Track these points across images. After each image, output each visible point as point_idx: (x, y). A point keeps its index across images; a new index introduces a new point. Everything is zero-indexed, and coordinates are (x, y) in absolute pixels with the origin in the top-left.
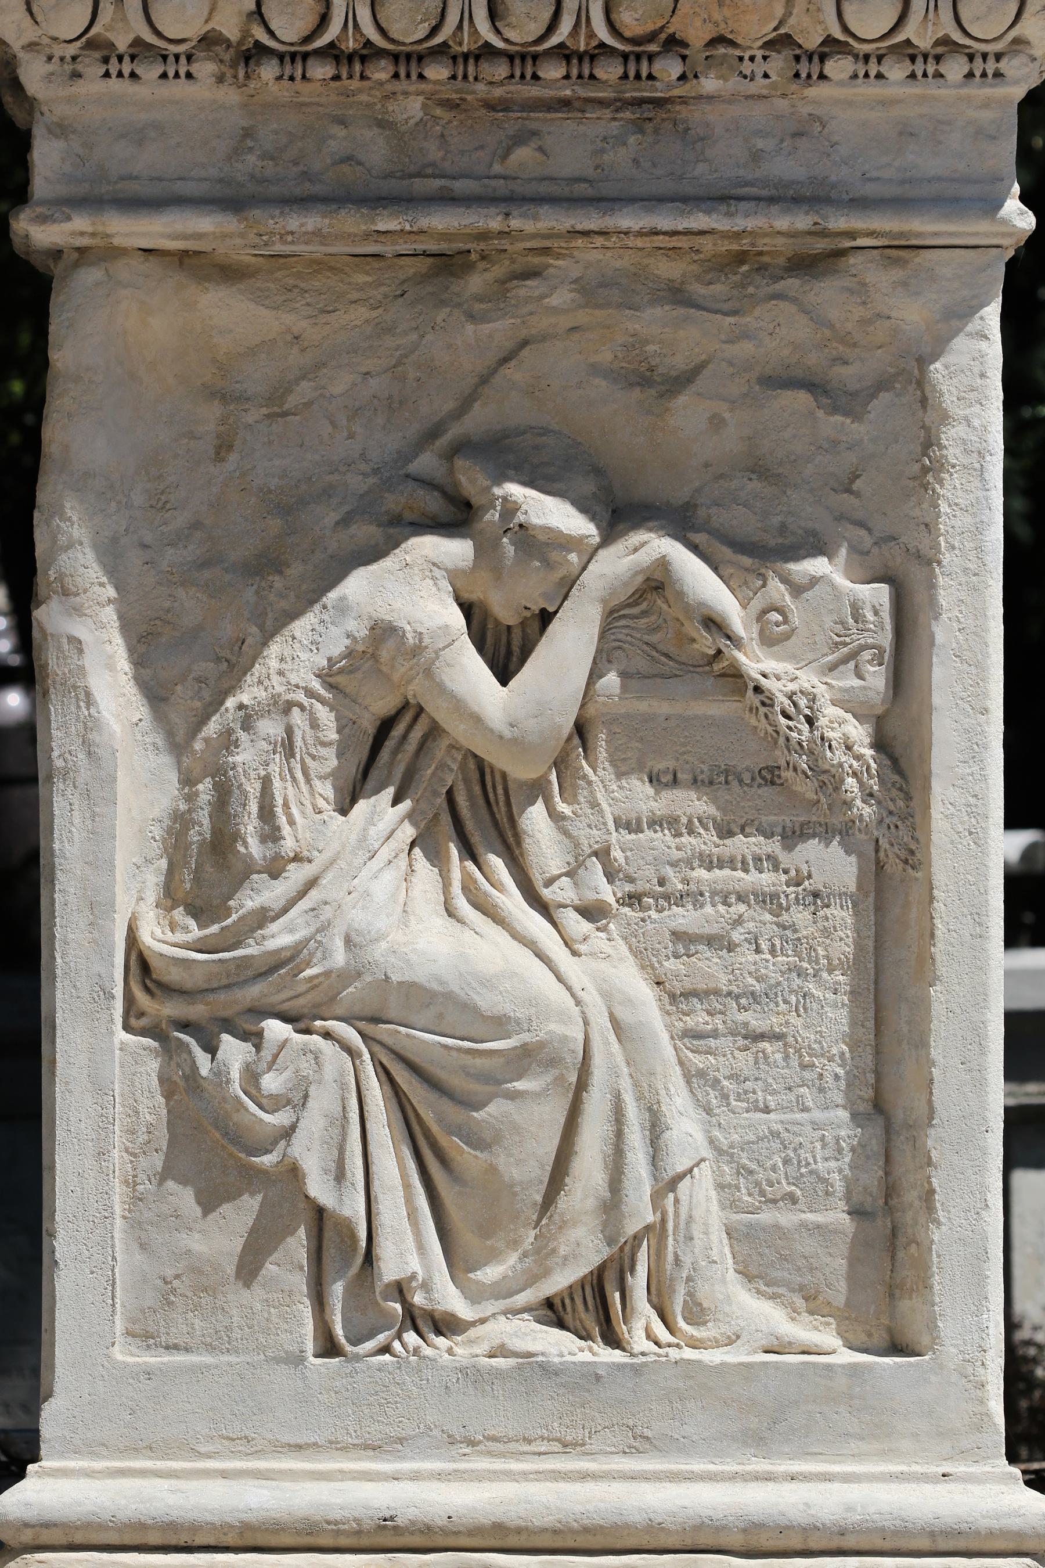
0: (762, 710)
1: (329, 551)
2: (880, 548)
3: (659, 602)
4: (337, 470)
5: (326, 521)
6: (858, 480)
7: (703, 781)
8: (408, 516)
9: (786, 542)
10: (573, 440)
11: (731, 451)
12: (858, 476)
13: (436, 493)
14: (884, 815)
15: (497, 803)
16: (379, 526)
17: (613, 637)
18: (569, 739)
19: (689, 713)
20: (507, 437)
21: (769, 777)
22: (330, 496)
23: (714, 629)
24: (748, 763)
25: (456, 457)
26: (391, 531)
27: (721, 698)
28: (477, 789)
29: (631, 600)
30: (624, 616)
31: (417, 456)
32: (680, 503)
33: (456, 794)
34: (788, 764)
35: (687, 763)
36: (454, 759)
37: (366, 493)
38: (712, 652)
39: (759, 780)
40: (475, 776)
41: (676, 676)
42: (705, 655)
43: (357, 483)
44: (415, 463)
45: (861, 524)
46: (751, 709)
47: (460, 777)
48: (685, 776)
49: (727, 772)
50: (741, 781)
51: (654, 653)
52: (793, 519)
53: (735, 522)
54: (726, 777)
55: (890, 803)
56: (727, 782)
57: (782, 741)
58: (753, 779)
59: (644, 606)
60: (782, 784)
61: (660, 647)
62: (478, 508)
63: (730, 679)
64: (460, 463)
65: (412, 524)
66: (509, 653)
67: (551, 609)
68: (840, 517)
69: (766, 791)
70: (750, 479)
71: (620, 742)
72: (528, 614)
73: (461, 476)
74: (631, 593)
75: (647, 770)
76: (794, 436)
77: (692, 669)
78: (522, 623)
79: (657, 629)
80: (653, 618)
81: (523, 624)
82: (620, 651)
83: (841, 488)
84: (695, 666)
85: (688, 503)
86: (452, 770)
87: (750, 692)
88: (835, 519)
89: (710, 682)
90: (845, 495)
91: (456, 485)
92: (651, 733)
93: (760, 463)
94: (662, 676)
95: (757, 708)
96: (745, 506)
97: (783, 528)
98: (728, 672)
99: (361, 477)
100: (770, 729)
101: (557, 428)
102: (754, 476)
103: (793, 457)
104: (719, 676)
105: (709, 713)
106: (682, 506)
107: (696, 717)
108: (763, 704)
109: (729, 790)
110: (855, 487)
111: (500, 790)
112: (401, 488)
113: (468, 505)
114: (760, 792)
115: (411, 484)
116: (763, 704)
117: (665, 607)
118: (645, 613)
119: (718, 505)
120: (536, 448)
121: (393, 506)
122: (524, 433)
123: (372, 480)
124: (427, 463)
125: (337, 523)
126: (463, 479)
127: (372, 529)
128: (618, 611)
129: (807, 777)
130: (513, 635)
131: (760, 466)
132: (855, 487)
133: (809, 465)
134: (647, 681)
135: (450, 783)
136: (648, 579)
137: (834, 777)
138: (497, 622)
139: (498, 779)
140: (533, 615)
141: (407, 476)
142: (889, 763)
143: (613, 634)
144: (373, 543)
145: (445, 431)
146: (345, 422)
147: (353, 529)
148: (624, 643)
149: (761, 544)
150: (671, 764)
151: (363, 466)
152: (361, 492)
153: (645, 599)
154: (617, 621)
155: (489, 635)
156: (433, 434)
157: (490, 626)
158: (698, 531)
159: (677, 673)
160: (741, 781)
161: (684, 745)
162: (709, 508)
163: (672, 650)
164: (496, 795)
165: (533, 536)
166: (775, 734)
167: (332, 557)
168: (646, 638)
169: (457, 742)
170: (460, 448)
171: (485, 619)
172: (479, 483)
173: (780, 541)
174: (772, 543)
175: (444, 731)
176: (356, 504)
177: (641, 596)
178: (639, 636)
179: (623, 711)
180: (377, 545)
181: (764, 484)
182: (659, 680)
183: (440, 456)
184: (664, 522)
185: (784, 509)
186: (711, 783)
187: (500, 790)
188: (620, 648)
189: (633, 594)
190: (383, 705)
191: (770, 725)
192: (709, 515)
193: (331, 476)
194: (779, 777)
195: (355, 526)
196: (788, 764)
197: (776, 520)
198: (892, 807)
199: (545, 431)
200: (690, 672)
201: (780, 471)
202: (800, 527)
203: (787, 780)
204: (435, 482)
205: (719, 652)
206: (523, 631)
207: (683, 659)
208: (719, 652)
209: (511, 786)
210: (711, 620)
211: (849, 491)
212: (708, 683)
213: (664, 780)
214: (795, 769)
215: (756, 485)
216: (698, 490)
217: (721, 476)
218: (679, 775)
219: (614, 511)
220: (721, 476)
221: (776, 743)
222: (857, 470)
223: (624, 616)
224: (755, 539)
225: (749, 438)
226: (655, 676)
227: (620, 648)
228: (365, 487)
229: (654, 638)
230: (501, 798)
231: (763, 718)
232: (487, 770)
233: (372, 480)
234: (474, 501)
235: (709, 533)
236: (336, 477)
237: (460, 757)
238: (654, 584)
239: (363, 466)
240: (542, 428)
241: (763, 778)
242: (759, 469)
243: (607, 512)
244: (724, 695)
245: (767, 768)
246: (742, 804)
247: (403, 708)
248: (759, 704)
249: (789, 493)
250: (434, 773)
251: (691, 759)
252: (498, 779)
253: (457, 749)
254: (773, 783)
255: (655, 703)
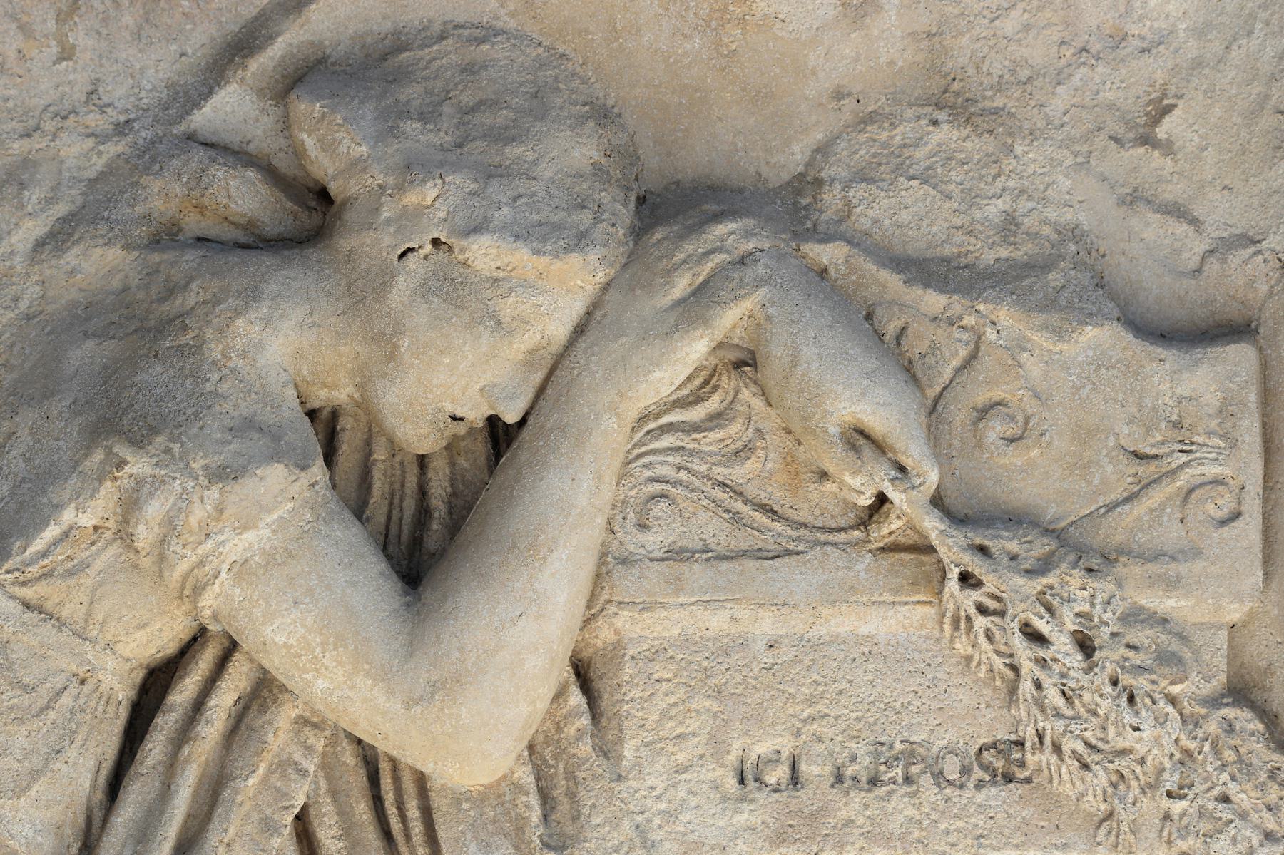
0: (981, 622)
1: (23, 305)
2: (1224, 260)
3: (746, 394)
4: (37, 128)
5: (14, 239)
6: (1167, 118)
7: (855, 778)
8: (194, 224)
9: (1018, 254)
10: (548, 49)
11: (892, 63)
12: (1168, 110)
13: (251, 174)
14: (1255, 842)
15: (408, 837)
16: (126, 247)
17: (648, 473)
18: (560, 695)
19: (820, 631)
20: (402, 48)
21: (1000, 764)
22: (23, 186)
23: (867, 451)
24: (949, 736)
25: (293, 96)
26: (156, 257)
27: (887, 597)
28: (363, 811)
29: (686, 392)
30: (670, 428)
31: (210, 93)
32: (785, 177)
33: (315, 823)
34: (1041, 737)
35: (820, 740)
36: (309, 749)
37: (102, 177)
38: (865, 500)
39: (978, 773)
40: (356, 780)
41: (789, 553)
42: (849, 506)
43: (77, 153)
44: (207, 109)
45: (1178, 212)
46: (956, 622)
47: (323, 785)
48: (816, 770)
49: (910, 756)
50: (939, 776)
51: (739, 506)
52: (1030, 205)
53: (904, 216)
54: (907, 766)
55: (1265, 813)
56: (908, 780)
57: (1027, 687)
58: (966, 770)
59: (714, 404)
60: (1029, 781)
61: (752, 491)
62: (344, 203)
63: (908, 557)
64: (305, 107)
65: (201, 240)
66: (424, 512)
67: (511, 418)
68: (1133, 199)
69: (995, 796)
70: (935, 123)
71: (672, 700)
72: (461, 429)
73: (305, 136)
74: (683, 377)
75: (732, 758)
76: (1027, 28)
77: (822, 537)
78: (448, 447)
79: (742, 453)
80: (735, 428)
81: (451, 447)
82: (663, 504)
83: (1131, 135)
84: (830, 530)
85: (802, 176)
86: (303, 773)
87: (953, 585)
88: (1121, 202)
89: (864, 562)
90: (1141, 150)
91: (299, 153)
92: (739, 678)
93: (956, 86)
94: (760, 555)
95: (968, 618)
96: (925, 182)
97: (1010, 225)
98: (902, 539)
99: (90, 143)
100: (998, 662)
101: (512, 24)
102: (941, 116)
103: (1024, 73)
104: (882, 549)
105: (864, 630)
106: (789, 183)
107: (834, 639)
108: (982, 610)
109: (913, 795)
110: (1161, 133)
111: (413, 812)
112: (176, 163)
113: (323, 195)
114: (980, 797)
115: (199, 154)
116: (982, 610)
117: (758, 403)
118: (717, 419)
119: (870, 181)
120: (470, 69)
121: (158, 204)
122: (442, 37)
123: (112, 149)
124: (233, 107)
125: (40, 244)
126: (309, 142)
127: (115, 254)
128: (658, 416)
129: (1085, 766)
130: (431, 474)
131: (957, 94)
132: (1161, 133)
133: (1060, 89)
134: (724, 566)
135: (300, 801)
136: (720, 345)
137: (1142, 761)
138: (394, 448)
139: (409, 787)
140: (472, 431)
141: (190, 137)
142: (1261, 727)
143: (649, 466)
144: (116, 283)
145: (271, 38)
146: (51, 25)
147: (71, 257)
148: (674, 484)
149: (963, 261)
150: (786, 745)
151: (95, 120)
152: (91, 174)
153: (716, 388)
154: (656, 438)
155: (377, 475)
156: (241, 46)
157: (379, 455)
158: (826, 239)
159: (791, 546)
160: (939, 776)
161: (810, 701)
162: (847, 187)
163: (778, 496)
164: (404, 819)
165: (465, 264)
166: (1010, 674)
167: (29, 318)
168: (721, 472)
169: (313, 711)
170: (303, 76)
171: (368, 442)
172: (342, 150)
173: (1003, 253)
174: (988, 257)
175: (283, 689)
176: (78, 203)
177: (706, 382)
178: (704, 468)
179: (676, 631)
180: (125, 289)
181: (965, 132)
182: (750, 564)
183: (261, 93)
184: (750, 222)
185: (1011, 184)
186: (874, 781)
187: (413, 812)
188: (663, 496)
189: (689, 379)
190: (157, 637)
191: (998, 653)
192: (848, 204)
193: (26, 141)
194: (1022, 764)
195: (76, 250)
196: (1041, 737)
197: (995, 209)
198: (1271, 825)
199: (487, 33)
200: (818, 543)
201: (998, 102)
202: (1045, 222)
203: (1039, 770)
204: (251, 148)
205: (882, 499)
206: (452, 464)
207: (802, 516)
208: (882, 499)
209: (438, 802)
210: (862, 433)
211: (1147, 140)
212: (861, 567)
213: (771, 779)
214: (1057, 749)
215: (945, 135)
216: (823, 150)
217: (871, 118)
218: (803, 767)
219: (641, 200)
220: (871, 118)
221: (1013, 690)
222: (1165, 95)
223: (670, 428)
224: (950, 250)
225: (930, 35)
226: (743, 554)
227: (663, 496)
228: (99, 164)
229: (739, 473)
230: (417, 828)
231: (982, 639)
232: (384, 767)
233: (112, 149)
234: (333, 188)
235: (849, 242)
236: (38, 142)
237: (320, 745)
238: (732, 356)
239: (95, 120)
240: (479, 26)
241: (986, 768)
242: (951, 101)
243: (625, 205)
244: (897, 591)
245: (994, 745)
246: (943, 827)
247: (195, 639)
248: (972, 611)
249: (1019, 149)
250: (265, 780)
251: (828, 732)
252: (409, 787)
253: (315, 726)
254: (1009, 778)
255: (744, 614)
